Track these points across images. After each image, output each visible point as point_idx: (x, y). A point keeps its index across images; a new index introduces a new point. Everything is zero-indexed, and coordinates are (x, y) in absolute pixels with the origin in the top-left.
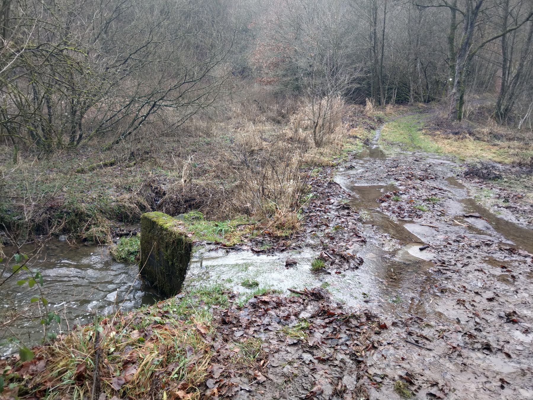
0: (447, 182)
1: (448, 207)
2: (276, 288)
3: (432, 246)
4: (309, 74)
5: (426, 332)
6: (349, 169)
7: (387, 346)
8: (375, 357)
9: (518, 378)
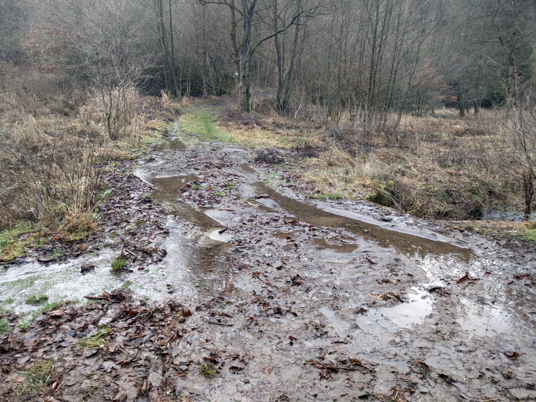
0: (240, 168)
1: (242, 191)
2: (70, 299)
3: (230, 229)
4: (96, 63)
5: (228, 310)
6: (149, 161)
7: (192, 332)
8: (180, 347)
9: (303, 332)
